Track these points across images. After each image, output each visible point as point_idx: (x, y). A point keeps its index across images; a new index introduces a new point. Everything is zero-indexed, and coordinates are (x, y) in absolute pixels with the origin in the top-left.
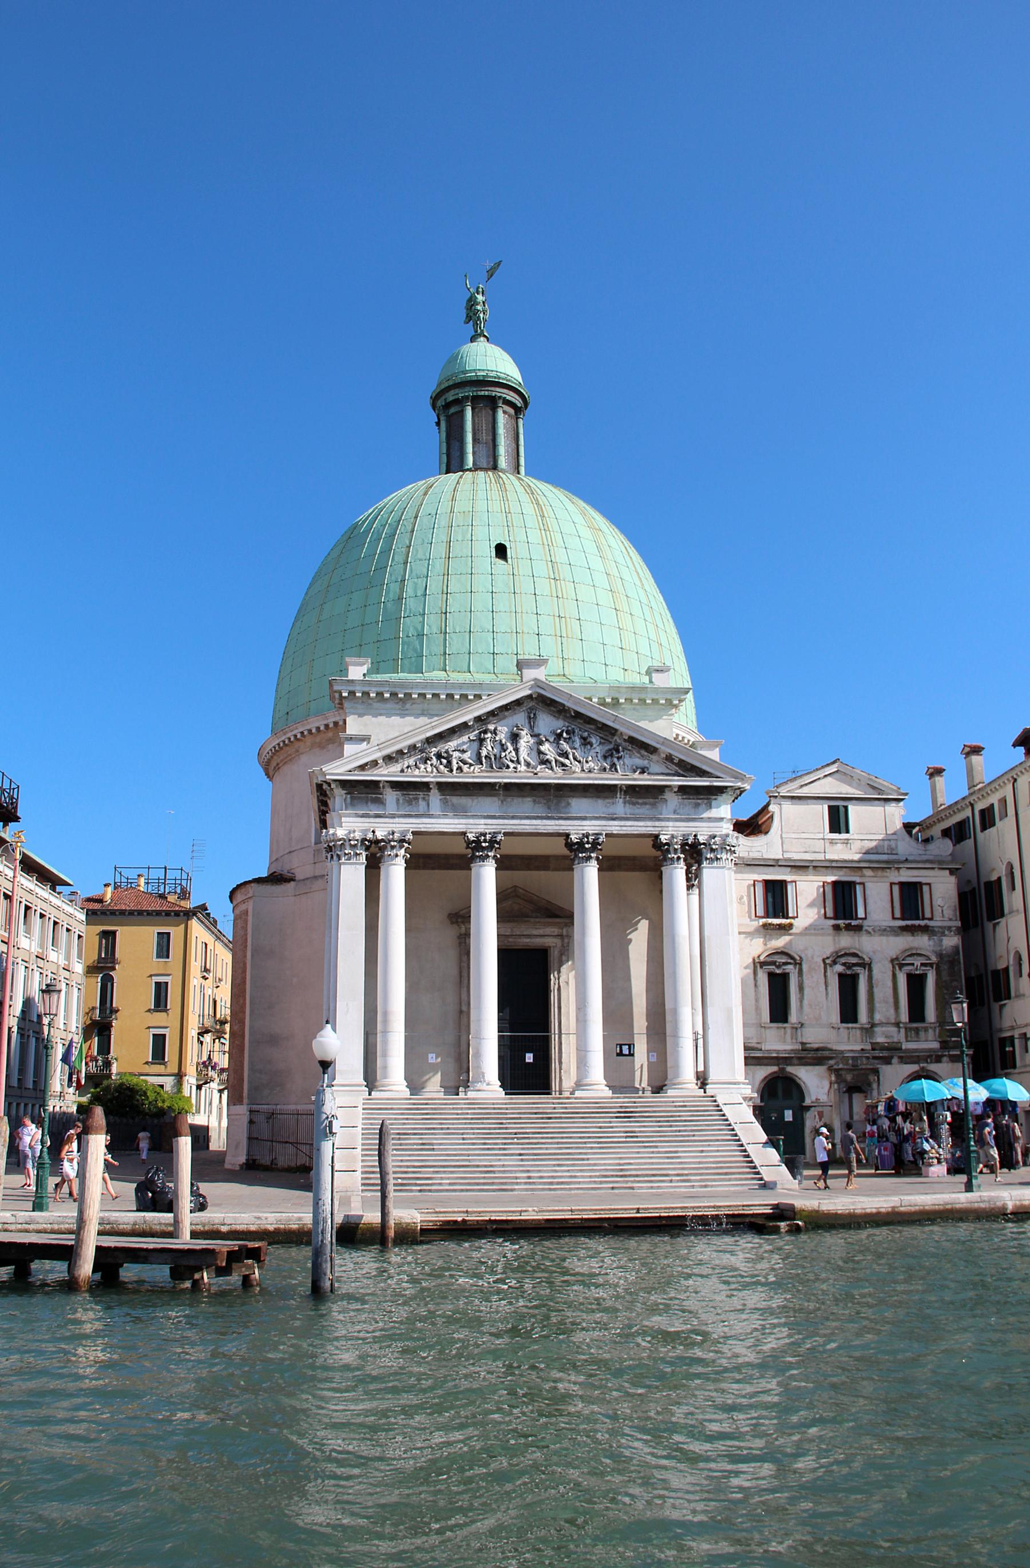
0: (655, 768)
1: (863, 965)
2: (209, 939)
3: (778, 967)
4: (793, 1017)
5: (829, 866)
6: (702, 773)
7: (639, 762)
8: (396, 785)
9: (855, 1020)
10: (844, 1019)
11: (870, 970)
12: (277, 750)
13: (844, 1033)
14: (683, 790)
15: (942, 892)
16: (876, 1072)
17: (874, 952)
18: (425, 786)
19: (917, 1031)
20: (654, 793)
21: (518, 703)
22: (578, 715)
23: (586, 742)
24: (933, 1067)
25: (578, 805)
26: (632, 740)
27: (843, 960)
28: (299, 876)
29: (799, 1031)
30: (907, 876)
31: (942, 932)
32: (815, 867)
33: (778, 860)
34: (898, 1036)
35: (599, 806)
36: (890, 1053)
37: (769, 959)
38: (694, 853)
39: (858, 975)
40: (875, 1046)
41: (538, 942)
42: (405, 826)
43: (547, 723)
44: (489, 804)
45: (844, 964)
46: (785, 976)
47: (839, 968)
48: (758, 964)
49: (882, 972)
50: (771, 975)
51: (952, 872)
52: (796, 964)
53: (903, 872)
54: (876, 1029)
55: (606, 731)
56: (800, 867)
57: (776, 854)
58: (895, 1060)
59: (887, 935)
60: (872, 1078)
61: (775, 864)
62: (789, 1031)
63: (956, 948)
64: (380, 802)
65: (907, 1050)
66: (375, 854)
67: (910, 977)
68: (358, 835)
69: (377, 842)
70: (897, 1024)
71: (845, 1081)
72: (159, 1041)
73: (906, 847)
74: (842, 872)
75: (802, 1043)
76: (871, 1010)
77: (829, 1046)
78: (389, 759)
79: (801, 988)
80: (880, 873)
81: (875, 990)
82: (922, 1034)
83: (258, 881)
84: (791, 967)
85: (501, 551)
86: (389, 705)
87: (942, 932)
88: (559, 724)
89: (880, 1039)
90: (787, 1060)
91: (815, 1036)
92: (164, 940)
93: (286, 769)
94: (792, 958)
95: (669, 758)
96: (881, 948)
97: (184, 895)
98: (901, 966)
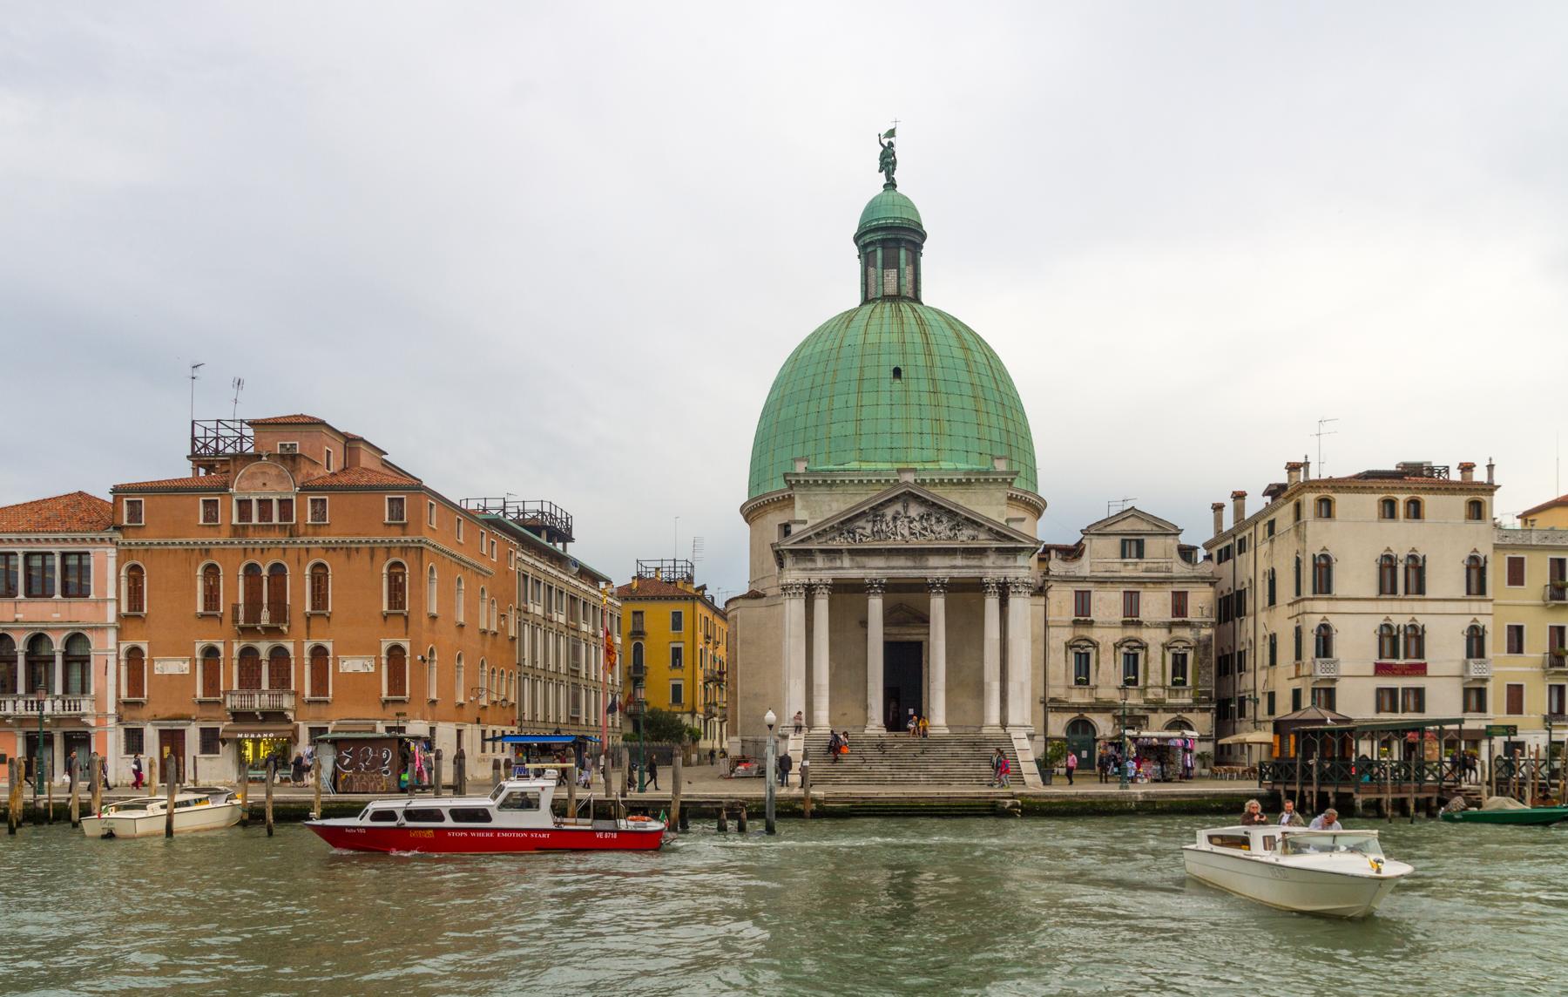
0: (982, 536)
2: (708, 614)
4: (1092, 683)
5: (1123, 581)
6: (1012, 539)
7: (971, 532)
8: (822, 551)
9: (1135, 682)
12: (752, 510)
14: (999, 550)
15: (1201, 600)
18: (840, 551)
20: (981, 552)
21: (897, 497)
22: (934, 504)
23: (939, 521)
25: (933, 561)
26: (967, 519)
28: (770, 593)
30: (1178, 588)
31: (1201, 625)
35: (947, 561)
38: (1004, 591)
41: (915, 638)
42: (827, 576)
43: (915, 511)
44: (879, 562)
46: (1087, 655)
47: (1125, 649)
48: (1069, 646)
49: (1155, 652)
51: (1212, 584)
55: (952, 514)
57: (1086, 572)
61: (1084, 579)
63: (1210, 638)
64: (813, 561)
66: (810, 591)
67: (1175, 655)
68: (801, 581)
69: (810, 585)
72: (677, 690)
76: (1146, 678)
78: (817, 535)
83: (743, 597)
86: (818, 490)
87: (1201, 625)
88: (923, 510)
92: (677, 617)
93: (758, 522)
95: (990, 529)
96: (1154, 638)
97: (690, 579)
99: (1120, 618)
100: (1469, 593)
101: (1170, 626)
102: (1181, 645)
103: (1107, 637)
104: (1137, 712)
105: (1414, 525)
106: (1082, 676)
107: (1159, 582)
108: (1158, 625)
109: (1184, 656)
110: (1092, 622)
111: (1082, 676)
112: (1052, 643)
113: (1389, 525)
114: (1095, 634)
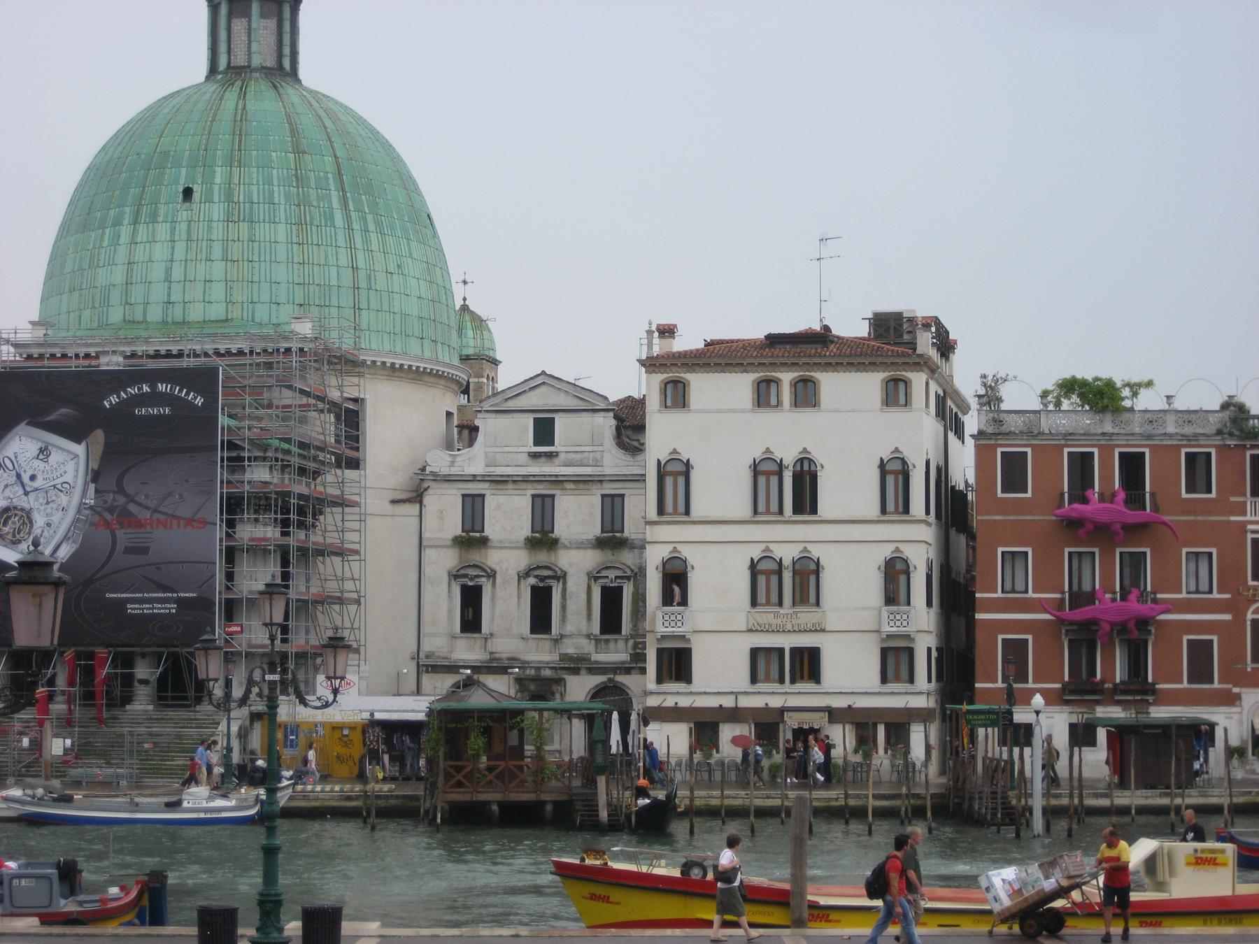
1: (557, 578)
3: (471, 579)
10: (534, 630)
11: (565, 583)
13: (532, 644)
16: (560, 681)
17: (570, 565)
19: (607, 641)
24: (621, 679)
27: (536, 573)
29: (489, 642)
30: (609, 489)
32: (514, 481)
33: (474, 476)
34: (588, 647)
36: (576, 665)
37: (462, 572)
39: (549, 589)
40: (564, 657)
45: (537, 577)
47: (532, 581)
48: (454, 576)
49: (577, 584)
50: (465, 590)
52: (488, 576)
53: (606, 485)
54: (565, 640)
56: (500, 482)
57: (478, 468)
58: (583, 672)
59: (585, 548)
60: (555, 688)
61: (474, 478)
62: (479, 643)
65: (597, 662)
67: (605, 590)
70: (588, 636)
71: (529, 690)
73: (613, 461)
74: (541, 486)
75: (491, 653)
76: (563, 619)
77: (518, 656)
79: (493, 599)
80: (581, 486)
81: (568, 601)
82: (612, 645)
84: (484, 579)
85: (188, 193)
89: (570, 651)
90: (476, 669)
91: (505, 646)
94: (484, 570)
98: (596, 579)
99: (526, 531)
100: (884, 510)
101: (600, 544)
102: (612, 574)
103: (508, 559)
104: (547, 673)
105: (805, 417)
106: (471, 622)
107: (583, 482)
108: (580, 545)
109: (620, 589)
110: (484, 542)
111: (471, 622)
112: (428, 570)
113: (767, 418)
114: (493, 558)
